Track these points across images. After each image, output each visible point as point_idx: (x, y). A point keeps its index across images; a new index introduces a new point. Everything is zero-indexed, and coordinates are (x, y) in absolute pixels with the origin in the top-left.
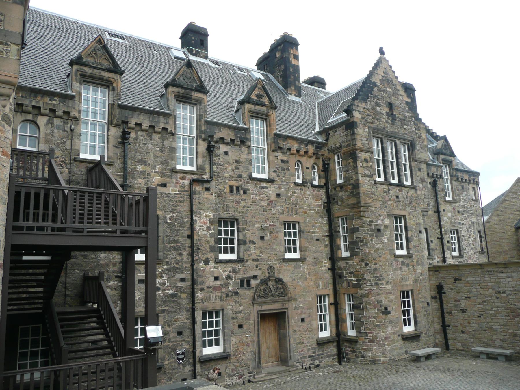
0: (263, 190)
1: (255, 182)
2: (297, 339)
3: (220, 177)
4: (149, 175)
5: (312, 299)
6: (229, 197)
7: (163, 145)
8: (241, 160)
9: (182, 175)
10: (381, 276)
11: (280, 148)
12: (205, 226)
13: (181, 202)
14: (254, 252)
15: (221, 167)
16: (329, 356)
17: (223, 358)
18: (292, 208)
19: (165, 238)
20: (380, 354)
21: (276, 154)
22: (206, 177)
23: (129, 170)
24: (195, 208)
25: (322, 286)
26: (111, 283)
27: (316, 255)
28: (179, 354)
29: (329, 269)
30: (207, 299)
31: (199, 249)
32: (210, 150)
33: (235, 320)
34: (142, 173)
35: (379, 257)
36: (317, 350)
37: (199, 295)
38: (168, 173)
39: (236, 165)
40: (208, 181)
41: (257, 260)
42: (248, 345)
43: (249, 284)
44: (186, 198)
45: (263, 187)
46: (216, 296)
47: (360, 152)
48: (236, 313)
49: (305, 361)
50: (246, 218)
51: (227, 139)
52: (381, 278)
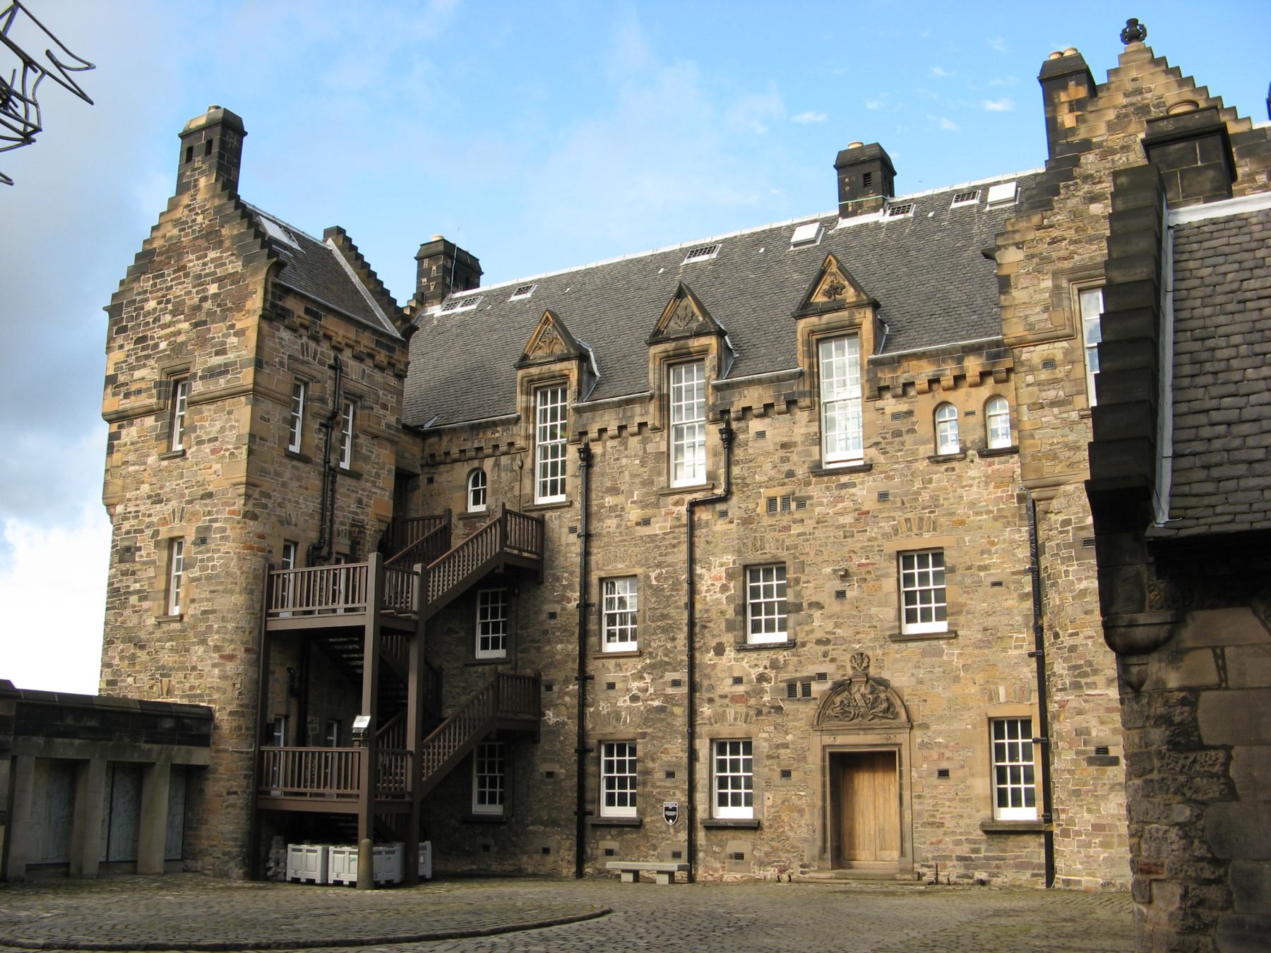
0: (843, 492)
1: (825, 479)
2: (926, 814)
3: (748, 485)
4: (623, 509)
5: (974, 727)
6: (767, 521)
7: (645, 452)
8: (794, 439)
9: (676, 497)
10: (1090, 664)
11: (887, 388)
12: (718, 584)
13: (674, 546)
14: (820, 624)
15: (752, 464)
16: (1021, 866)
17: (752, 827)
18: (921, 519)
19: (648, 613)
20: (1079, 866)
21: (879, 404)
22: (720, 491)
23: (594, 509)
24: (698, 553)
25: (1007, 695)
26: (571, 687)
27: (990, 622)
28: (667, 809)
29: (1031, 655)
30: (720, 718)
31: (705, 627)
32: (729, 438)
33: (775, 761)
34: (612, 509)
35: (1086, 613)
36: (983, 847)
37: (705, 710)
38: (653, 499)
39: (782, 453)
40: (724, 499)
41: (827, 642)
42: (801, 811)
43: (807, 691)
44: (684, 538)
45: (844, 486)
46: (736, 713)
47: (1025, 350)
48: (778, 746)
49: (945, 867)
50: (802, 558)
51: (757, 407)
52: (1089, 670)
